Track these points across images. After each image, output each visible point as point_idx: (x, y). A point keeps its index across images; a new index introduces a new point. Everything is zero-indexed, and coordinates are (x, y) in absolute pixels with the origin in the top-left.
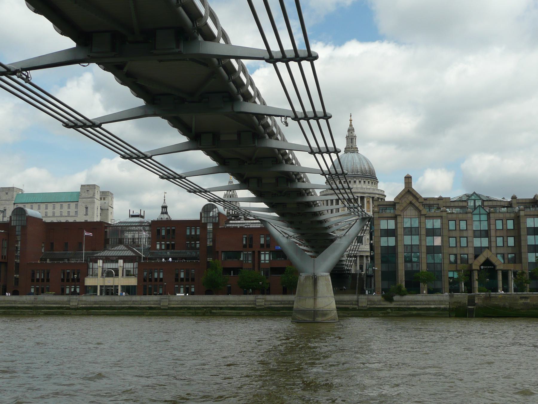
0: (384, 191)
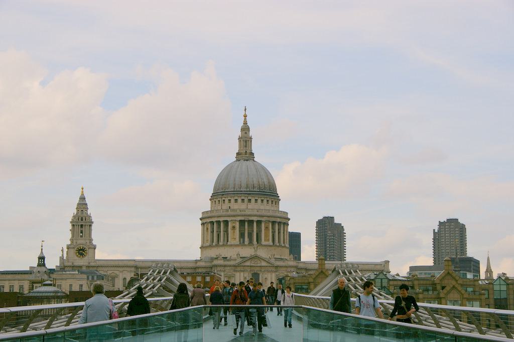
0: (287, 213)
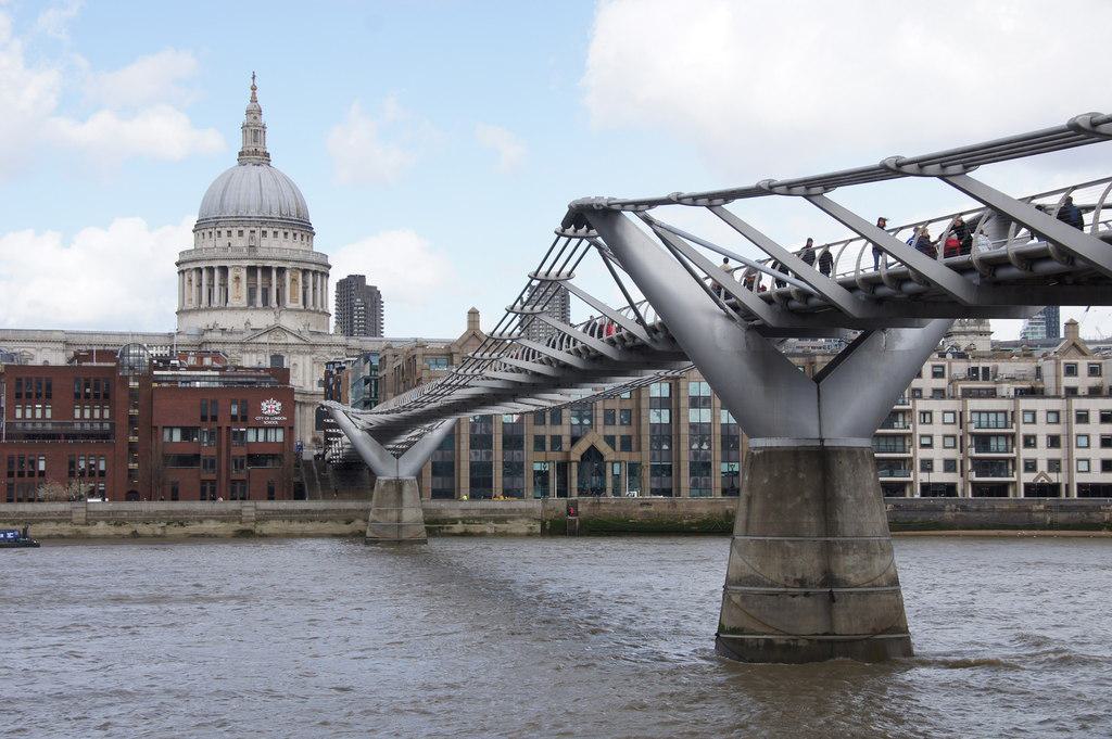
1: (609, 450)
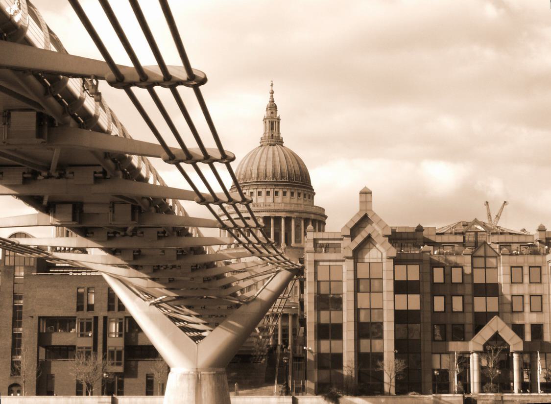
0: (323, 210)
1: (517, 339)
